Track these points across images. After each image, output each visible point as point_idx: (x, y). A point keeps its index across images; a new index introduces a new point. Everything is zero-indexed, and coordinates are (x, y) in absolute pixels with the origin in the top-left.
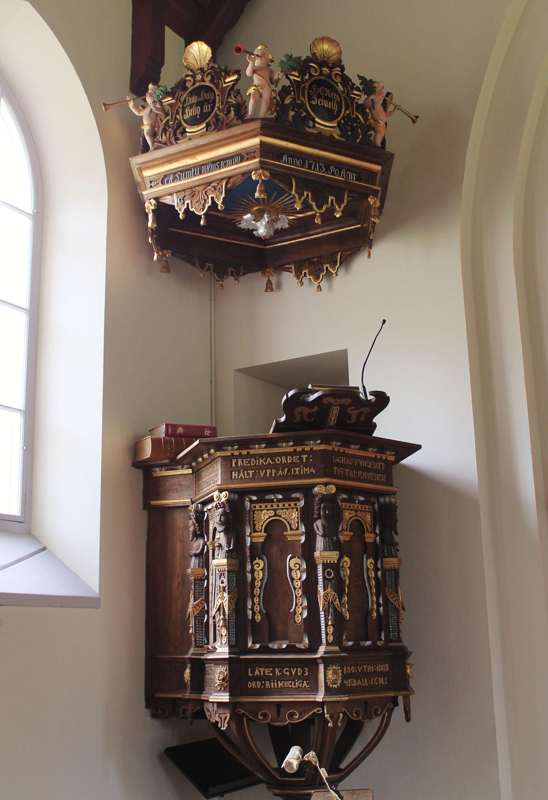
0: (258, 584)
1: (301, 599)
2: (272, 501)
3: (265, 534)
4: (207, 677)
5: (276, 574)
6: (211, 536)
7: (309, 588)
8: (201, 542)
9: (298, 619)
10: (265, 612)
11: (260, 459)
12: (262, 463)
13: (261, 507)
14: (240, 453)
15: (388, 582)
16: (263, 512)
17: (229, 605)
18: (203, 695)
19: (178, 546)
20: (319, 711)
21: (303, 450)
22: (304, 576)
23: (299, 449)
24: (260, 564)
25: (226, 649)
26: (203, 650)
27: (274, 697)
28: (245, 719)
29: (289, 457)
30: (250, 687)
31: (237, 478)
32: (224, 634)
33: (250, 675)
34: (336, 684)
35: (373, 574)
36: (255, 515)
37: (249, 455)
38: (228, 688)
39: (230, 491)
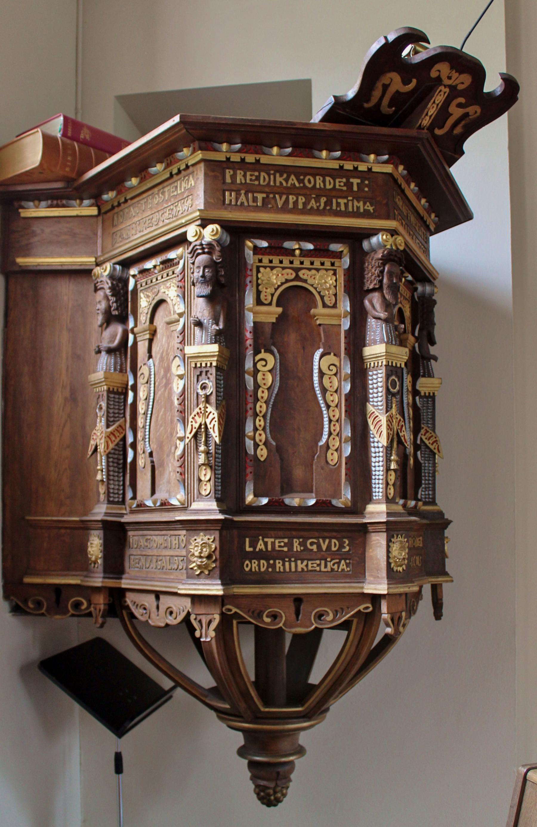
0: (263, 394)
1: (337, 425)
2: (290, 252)
3: (280, 310)
4: (128, 552)
8: (119, 329)
9: (333, 457)
10: (274, 444)
11: (278, 175)
12: (281, 183)
14: (243, 160)
16: (275, 271)
18: (123, 581)
19: (64, 339)
20: (367, 608)
21: (356, 169)
22: (347, 388)
23: (349, 166)
24: (269, 361)
25: (213, 505)
27: (292, 585)
28: (235, 622)
29: (328, 179)
30: (247, 569)
31: (233, 203)
33: (248, 549)
34: (401, 566)
36: (260, 275)
38: (217, 572)
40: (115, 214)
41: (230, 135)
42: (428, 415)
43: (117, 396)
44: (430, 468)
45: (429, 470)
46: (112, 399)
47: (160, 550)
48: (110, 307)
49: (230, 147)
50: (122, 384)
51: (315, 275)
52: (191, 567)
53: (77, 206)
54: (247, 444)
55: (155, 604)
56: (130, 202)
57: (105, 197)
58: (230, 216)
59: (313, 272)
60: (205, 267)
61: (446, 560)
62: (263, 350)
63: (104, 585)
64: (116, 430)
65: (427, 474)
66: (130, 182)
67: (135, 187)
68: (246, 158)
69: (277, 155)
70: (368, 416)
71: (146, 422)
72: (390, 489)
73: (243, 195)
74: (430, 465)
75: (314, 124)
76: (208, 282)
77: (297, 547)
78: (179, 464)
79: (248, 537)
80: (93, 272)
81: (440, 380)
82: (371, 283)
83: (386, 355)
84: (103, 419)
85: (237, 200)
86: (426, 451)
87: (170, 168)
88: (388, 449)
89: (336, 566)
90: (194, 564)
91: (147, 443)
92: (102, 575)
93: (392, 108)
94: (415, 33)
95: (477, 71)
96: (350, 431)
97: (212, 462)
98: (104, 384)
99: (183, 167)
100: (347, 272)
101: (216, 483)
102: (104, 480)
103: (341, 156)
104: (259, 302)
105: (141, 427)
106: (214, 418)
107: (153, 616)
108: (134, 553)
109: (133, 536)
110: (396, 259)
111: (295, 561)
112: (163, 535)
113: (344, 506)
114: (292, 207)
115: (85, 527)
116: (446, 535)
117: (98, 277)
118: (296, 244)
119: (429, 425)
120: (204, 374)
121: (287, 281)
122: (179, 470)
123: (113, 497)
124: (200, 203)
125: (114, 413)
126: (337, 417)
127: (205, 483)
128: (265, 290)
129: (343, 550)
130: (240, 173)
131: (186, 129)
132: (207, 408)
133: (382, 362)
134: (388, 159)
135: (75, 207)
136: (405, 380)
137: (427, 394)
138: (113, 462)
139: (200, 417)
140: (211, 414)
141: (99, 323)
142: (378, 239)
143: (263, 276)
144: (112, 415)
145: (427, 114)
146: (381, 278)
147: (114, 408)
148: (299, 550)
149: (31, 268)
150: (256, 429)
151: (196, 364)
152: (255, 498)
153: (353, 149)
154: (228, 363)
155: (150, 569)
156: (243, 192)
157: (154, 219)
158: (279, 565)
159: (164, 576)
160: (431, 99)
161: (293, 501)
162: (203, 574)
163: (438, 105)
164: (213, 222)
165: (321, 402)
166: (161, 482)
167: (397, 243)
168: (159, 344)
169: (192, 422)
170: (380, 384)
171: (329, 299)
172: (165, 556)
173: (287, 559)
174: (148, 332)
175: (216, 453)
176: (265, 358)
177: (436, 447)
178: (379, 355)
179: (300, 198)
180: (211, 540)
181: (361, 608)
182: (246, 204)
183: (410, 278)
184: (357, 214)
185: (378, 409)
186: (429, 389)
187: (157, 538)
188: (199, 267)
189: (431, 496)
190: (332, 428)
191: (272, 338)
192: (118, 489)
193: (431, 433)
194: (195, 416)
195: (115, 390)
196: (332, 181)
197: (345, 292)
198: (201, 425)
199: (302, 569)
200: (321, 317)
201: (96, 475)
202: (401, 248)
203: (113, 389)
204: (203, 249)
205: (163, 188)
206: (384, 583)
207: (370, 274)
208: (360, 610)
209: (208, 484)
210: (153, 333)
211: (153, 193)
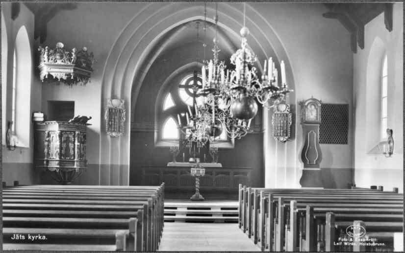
7: (74, 149)
8: (48, 138)
115: (44, 161)
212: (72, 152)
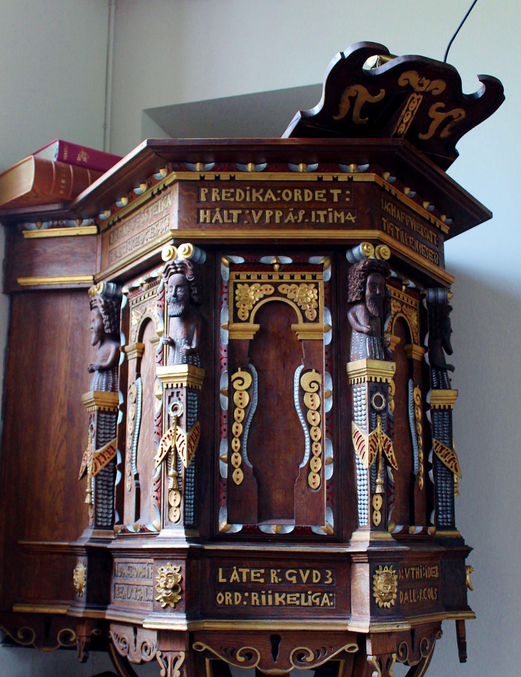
0: (239, 414)
1: (320, 446)
2: (270, 268)
3: (257, 326)
4: (117, 580)
5: (273, 400)
6: (134, 335)
7: (339, 424)
8: (111, 347)
9: (314, 481)
10: (251, 466)
11: (254, 191)
12: (257, 198)
13: (249, 277)
14: (217, 178)
15: (438, 426)
16: (253, 287)
17: (188, 451)
18: (108, 612)
20: (353, 648)
22: (329, 405)
23: (328, 177)
24: (246, 379)
25: (181, 533)
26: (109, 534)
28: (207, 661)
29: (306, 191)
30: (220, 602)
31: (208, 221)
32: (174, 504)
33: (221, 580)
34: (388, 601)
35: (420, 413)
36: (237, 292)
37: (232, 183)
38: (183, 605)
39: (198, 243)
40: (111, 233)
41: (207, 153)
42: (444, 430)
43: (109, 416)
44: (448, 489)
45: (447, 491)
46: (103, 419)
47: (139, 579)
48: (103, 325)
49: (204, 166)
50: (113, 403)
51: (295, 289)
52: (157, 599)
53: (77, 226)
54: (220, 467)
55: (133, 637)
56: (123, 221)
57: (102, 216)
58: (203, 234)
59: (293, 286)
60: (177, 287)
61: (469, 593)
62: (239, 369)
63: (85, 616)
64: (106, 451)
65: (444, 496)
66: (120, 202)
67: (125, 206)
68: (221, 176)
69: (252, 172)
70: (353, 436)
71: (133, 443)
72: (376, 515)
73: (218, 212)
74: (448, 485)
75: (284, 140)
76: (180, 301)
77: (274, 578)
78: (155, 488)
79: (221, 567)
80: (89, 291)
81: (456, 392)
82: (353, 295)
83: (367, 371)
84: (93, 439)
85: (212, 217)
86: (442, 470)
87: (151, 189)
88: (373, 470)
89: (318, 599)
90: (160, 596)
91: (134, 465)
92: (84, 605)
93: (365, 118)
94: (372, 47)
95: (450, 76)
96: (332, 452)
97: (182, 486)
98: (94, 403)
99: (161, 187)
100: (328, 285)
101: (187, 509)
102: (93, 503)
103: (318, 168)
104: (236, 319)
105: (129, 448)
106: (184, 441)
107: (132, 650)
108: (119, 582)
109: (119, 563)
110: (380, 269)
111: (273, 594)
112: (142, 563)
113: (326, 534)
114: (269, 222)
116: (467, 564)
117: (94, 296)
118: (274, 259)
119: (446, 441)
120: (175, 395)
121: (265, 296)
122: (155, 494)
123: (101, 521)
124: (174, 223)
125: (104, 433)
126: (319, 437)
127: (175, 509)
128: (242, 306)
129: (326, 582)
130: (216, 191)
131: (155, 153)
132: (177, 430)
133: (364, 378)
134: (369, 167)
135: (74, 226)
136: (410, 393)
137: (442, 408)
138: (102, 484)
139: (170, 440)
140: (181, 436)
141: (92, 342)
142: (359, 249)
143: (240, 292)
144: (102, 436)
145: (402, 122)
146: (363, 290)
147: (104, 428)
148: (277, 581)
149: (33, 288)
150: (231, 452)
151: (167, 385)
152: (229, 525)
153: (330, 161)
154: (203, 383)
155: (131, 600)
156: (218, 209)
157: (140, 238)
158: (254, 597)
159: (142, 608)
160: (404, 106)
161: (270, 528)
162: (169, 607)
163: (413, 112)
164: (186, 241)
165: (302, 421)
166: (145, 507)
167: (381, 253)
168: (147, 363)
169: (162, 445)
170: (363, 402)
171: (310, 313)
172: (143, 586)
173: (263, 592)
174: (136, 350)
175: (186, 477)
176: (242, 377)
177: (454, 465)
178: (361, 371)
179: (277, 212)
180: (178, 570)
181: (346, 647)
182: (221, 221)
183: (412, 284)
184: (337, 226)
185: (362, 428)
186: (444, 402)
187: (139, 565)
188: (171, 287)
189: (449, 520)
190: (314, 449)
191: (249, 356)
192: (107, 513)
193: (447, 450)
194: (166, 438)
195: (107, 410)
196: (311, 193)
197: (325, 306)
198: (170, 448)
199: (280, 602)
200: (302, 333)
201: (84, 498)
202: (387, 258)
203: (104, 409)
204: (176, 268)
205: (148, 207)
206: (367, 621)
207: (353, 286)
208: (344, 650)
209: (178, 510)
210: (142, 351)
211: (140, 213)
212: (319, 467)
